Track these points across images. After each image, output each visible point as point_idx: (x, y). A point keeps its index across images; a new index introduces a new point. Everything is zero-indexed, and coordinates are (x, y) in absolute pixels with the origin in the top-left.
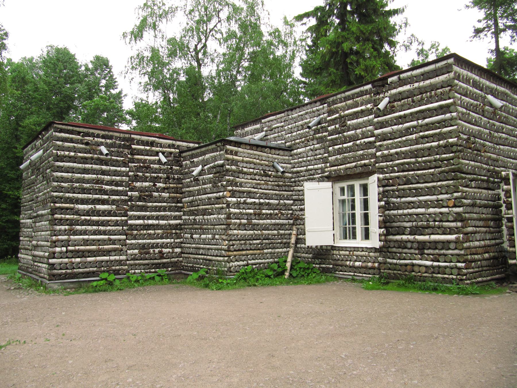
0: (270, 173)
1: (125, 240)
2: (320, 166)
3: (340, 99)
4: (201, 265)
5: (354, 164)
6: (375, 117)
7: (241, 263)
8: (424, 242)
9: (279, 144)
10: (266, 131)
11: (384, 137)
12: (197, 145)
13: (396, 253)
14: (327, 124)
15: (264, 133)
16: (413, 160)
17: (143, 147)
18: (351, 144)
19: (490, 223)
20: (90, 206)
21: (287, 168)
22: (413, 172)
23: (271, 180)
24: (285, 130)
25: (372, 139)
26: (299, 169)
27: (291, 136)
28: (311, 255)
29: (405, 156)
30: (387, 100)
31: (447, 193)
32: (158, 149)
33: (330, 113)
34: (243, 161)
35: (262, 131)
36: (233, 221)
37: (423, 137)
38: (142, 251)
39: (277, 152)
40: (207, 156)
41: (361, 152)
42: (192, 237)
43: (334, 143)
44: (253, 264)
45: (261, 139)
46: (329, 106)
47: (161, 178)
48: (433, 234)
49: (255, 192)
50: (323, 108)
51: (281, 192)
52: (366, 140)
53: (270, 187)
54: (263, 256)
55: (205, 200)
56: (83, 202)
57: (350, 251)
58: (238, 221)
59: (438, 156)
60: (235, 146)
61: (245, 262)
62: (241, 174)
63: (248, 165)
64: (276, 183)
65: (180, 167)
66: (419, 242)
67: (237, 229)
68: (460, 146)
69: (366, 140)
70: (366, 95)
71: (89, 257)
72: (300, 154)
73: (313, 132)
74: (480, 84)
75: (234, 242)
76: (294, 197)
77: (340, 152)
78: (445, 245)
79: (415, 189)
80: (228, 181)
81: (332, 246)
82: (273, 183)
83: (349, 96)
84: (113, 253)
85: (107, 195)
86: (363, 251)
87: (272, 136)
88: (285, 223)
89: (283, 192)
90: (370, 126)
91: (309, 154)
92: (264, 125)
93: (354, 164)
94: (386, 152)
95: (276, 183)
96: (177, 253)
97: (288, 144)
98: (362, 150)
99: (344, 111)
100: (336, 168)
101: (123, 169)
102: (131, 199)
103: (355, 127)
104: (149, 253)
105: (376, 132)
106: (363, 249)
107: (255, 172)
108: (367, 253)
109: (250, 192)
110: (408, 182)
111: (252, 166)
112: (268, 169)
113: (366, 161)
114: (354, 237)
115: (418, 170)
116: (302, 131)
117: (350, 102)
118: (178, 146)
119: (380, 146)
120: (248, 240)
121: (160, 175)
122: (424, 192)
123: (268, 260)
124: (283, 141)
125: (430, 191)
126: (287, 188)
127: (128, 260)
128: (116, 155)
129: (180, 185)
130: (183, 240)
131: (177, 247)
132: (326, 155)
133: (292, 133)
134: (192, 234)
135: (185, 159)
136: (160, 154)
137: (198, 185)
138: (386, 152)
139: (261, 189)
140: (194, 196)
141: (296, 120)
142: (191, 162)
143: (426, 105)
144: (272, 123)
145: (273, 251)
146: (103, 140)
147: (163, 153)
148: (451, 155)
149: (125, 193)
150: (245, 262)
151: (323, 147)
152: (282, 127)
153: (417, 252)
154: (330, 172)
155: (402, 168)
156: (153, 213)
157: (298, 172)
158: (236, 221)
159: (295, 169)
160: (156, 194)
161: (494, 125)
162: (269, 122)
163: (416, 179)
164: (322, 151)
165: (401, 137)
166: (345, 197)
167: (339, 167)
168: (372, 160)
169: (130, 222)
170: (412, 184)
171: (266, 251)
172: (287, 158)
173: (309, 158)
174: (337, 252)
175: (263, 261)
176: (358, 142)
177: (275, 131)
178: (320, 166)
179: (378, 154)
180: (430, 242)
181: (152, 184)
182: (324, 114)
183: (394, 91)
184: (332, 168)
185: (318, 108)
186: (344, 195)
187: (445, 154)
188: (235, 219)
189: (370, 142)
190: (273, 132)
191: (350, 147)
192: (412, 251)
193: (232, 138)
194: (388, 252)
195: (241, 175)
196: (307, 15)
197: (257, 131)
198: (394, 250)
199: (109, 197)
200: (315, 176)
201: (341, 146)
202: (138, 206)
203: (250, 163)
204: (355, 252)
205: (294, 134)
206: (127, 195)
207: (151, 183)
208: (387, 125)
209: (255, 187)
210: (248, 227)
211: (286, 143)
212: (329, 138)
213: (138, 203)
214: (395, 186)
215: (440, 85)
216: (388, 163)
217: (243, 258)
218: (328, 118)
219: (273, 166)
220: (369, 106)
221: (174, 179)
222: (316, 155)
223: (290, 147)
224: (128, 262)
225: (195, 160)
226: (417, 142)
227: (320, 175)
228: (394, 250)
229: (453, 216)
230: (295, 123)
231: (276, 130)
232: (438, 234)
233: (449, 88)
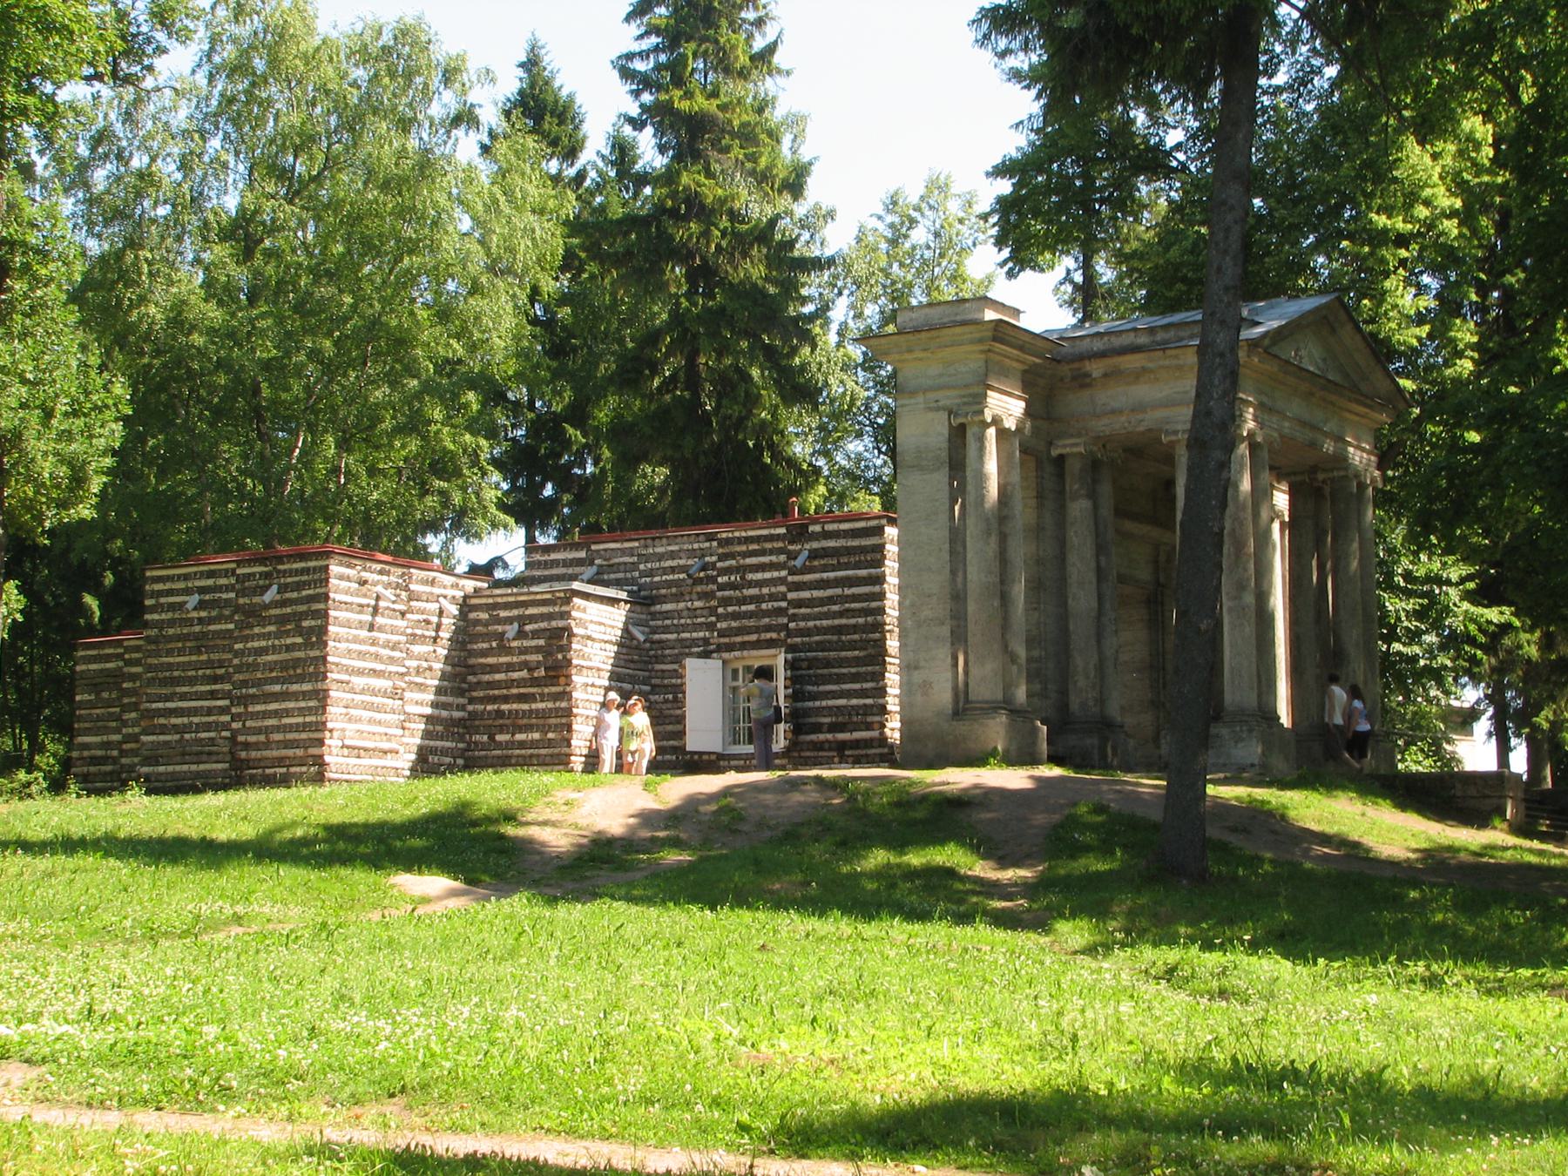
2: (701, 634)
11: (799, 603)
25: (784, 604)
33: (722, 557)
35: (592, 563)
37: (847, 610)
43: (726, 602)
52: (776, 604)
56: (360, 672)
69: (776, 604)
77: (735, 616)
94: (802, 624)
103: (760, 584)
105: (791, 596)
117: (755, 547)
125: (855, 678)
138: (802, 624)
155: (821, 646)
159: (656, 637)
164: (705, 612)
176: (764, 606)
178: (701, 634)
179: (792, 625)
183: (815, 545)
198: (808, 754)
205: (657, 579)
225: (503, 614)
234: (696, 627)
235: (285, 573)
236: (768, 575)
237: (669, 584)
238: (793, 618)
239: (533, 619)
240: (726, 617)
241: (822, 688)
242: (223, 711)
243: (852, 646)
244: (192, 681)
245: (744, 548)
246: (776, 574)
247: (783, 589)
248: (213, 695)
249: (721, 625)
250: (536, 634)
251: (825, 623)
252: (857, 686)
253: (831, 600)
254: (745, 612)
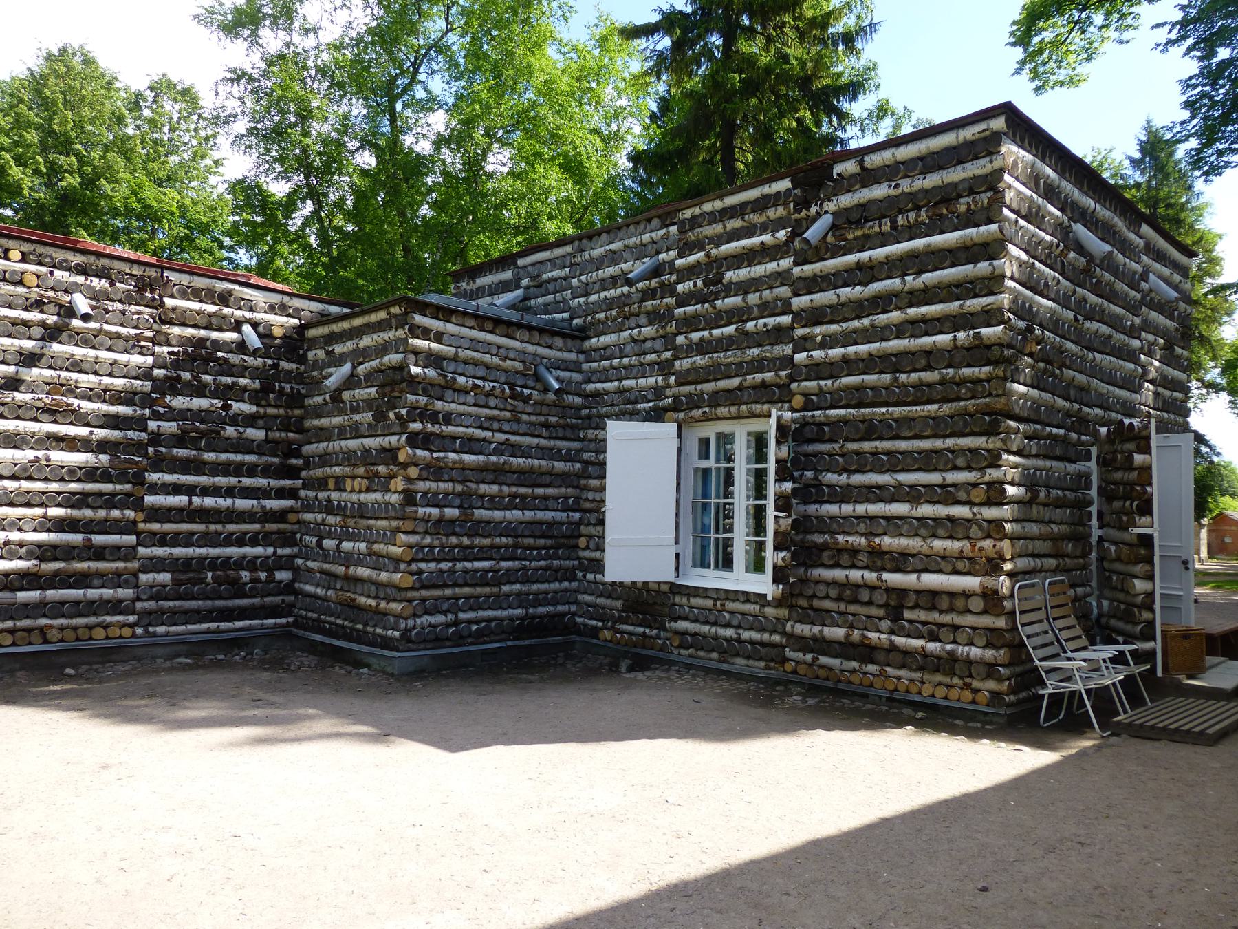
0: (527, 392)
1: (134, 548)
2: (651, 381)
3: (712, 213)
4: (338, 617)
5: (736, 382)
6: (796, 264)
7: (440, 619)
8: (902, 592)
9: (553, 321)
10: (527, 288)
11: (816, 316)
12: (346, 310)
13: (828, 611)
14: (674, 277)
15: (520, 292)
16: (887, 378)
17: (196, 306)
18: (730, 330)
19: (1067, 546)
20: (31, 454)
21: (570, 382)
22: (884, 410)
23: (529, 410)
24: (571, 287)
25: (786, 320)
26: (600, 386)
27: (587, 304)
28: (619, 604)
29: (866, 367)
30: (826, 220)
31: (969, 468)
32: (238, 313)
33: (686, 248)
34: (455, 359)
35: (518, 287)
36: (421, 511)
37: (913, 322)
38: (183, 577)
39: (548, 340)
40: (366, 341)
41: (755, 351)
42: (319, 544)
43: (690, 324)
44: (470, 622)
45: (513, 307)
46: (682, 231)
47: (244, 389)
48: (927, 570)
49: (484, 440)
50: (666, 237)
51: (553, 442)
52: (771, 321)
53: (524, 428)
54: (499, 602)
55: (355, 452)
57: (715, 600)
58: (435, 511)
59: (950, 371)
60: (436, 318)
61: (450, 617)
62: (450, 392)
63: (470, 369)
64: (542, 419)
65: (301, 364)
66: (890, 590)
67: (433, 531)
68: (1009, 346)
69: (771, 321)
70: (775, 205)
71: (22, 589)
72: (604, 349)
73: (640, 295)
74: (1060, 193)
75: (423, 565)
76: (585, 456)
77: (703, 348)
79: (887, 453)
80: (413, 408)
81: (672, 584)
82: (533, 418)
83: (733, 207)
84: (96, 582)
85: (88, 425)
86: (747, 601)
87: (540, 300)
88: (558, 519)
89: (559, 443)
90: (782, 285)
91: (628, 349)
92: (522, 272)
93: (736, 382)
94: (817, 354)
95: (542, 419)
96: (280, 582)
97: (575, 322)
98: (760, 345)
99: (717, 245)
100: (689, 389)
101: (137, 359)
102: (156, 439)
104: (202, 581)
106: (747, 597)
107: (487, 388)
108: (758, 607)
109: (471, 439)
110: (871, 430)
111: (481, 372)
112: (519, 383)
113: (769, 376)
114: (727, 563)
115: (898, 404)
116: (612, 292)
118: (297, 309)
119: (804, 338)
120: (460, 560)
121: (243, 381)
122: (909, 460)
123: (510, 612)
124: (566, 315)
125: (927, 461)
126: (568, 433)
127: (139, 599)
128: (117, 321)
129: (297, 412)
130: (300, 550)
131: (280, 568)
132: (668, 354)
133: (587, 294)
134: (321, 538)
135: (313, 343)
136: (247, 328)
137: (341, 412)
138: (817, 354)
139: (500, 431)
140: (328, 440)
141: (599, 264)
142: (327, 353)
143: (927, 236)
144: (542, 268)
145: (525, 588)
146: (80, 279)
147: (255, 325)
148: (986, 369)
149: (140, 424)
150: (450, 617)
151: (661, 332)
152: (565, 279)
153: (881, 613)
154: (676, 398)
155: (858, 397)
156: (217, 479)
157: (597, 394)
158: (429, 510)
159: (591, 387)
160: (230, 431)
161: (1085, 300)
162: (533, 265)
163: (890, 426)
164: (658, 344)
165: (858, 317)
166: (711, 463)
167: (699, 387)
168: (783, 373)
169: (149, 500)
170: (880, 438)
171: (506, 588)
172: (573, 356)
173: (625, 360)
174: (684, 600)
175: (498, 613)
176: (750, 325)
177: (547, 289)
178: (651, 381)
179: (800, 357)
180: (918, 592)
181: (218, 403)
182: (668, 249)
183: (846, 200)
184: (682, 389)
185: (653, 234)
186: (707, 457)
187: (969, 366)
188: (428, 505)
189: (778, 329)
190: (543, 290)
191: (730, 337)
192: (874, 611)
193: (434, 299)
194: (811, 608)
195: (449, 394)
196: (646, 31)
197: (505, 287)
198: (827, 604)
199: (91, 432)
200: (638, 406)
201: (706, 333)
202: (175, 459)
203: (476, 363)
204: (727, 603)
205: (594, 298)
206: (145, 430)
207: (214, 401)
208: (825, 285)
209: (485, 425)
210: (460, 526)
211: (572, 318)
212: (677, 311)
213: (175, 450)
214: (836, 442)
215: (966, 185)
216: (822, 383)
217: (445, 606)
218: (679, 262)
219: (537, 377)
220: (782, 234)
221: (281, 392)
222: (645, 353)
223: (582, 329)
224: (139, 605)
225: (339, 349)
226: (900, 330)
227: (651, 404)
228: (827, 604)
229: (980, 527)
230: (598, 269)
231: (551, 287)
232: (939, 571)
233: (989, 194)
234: (643, 370)
236: (758, 270)
237: (609, 304)
238: (803, 344)
239: (361, 355)
240: (690, 349)
241: (857, 479)
243: (922, 394)
245: (717, 228)
246: (772, 266)
247: (784, 291)
249: (682, 364)
250: (369, 378)
251: (863, 349)
252: (934, 478)
253: (882, 303)
254: (720, 340)
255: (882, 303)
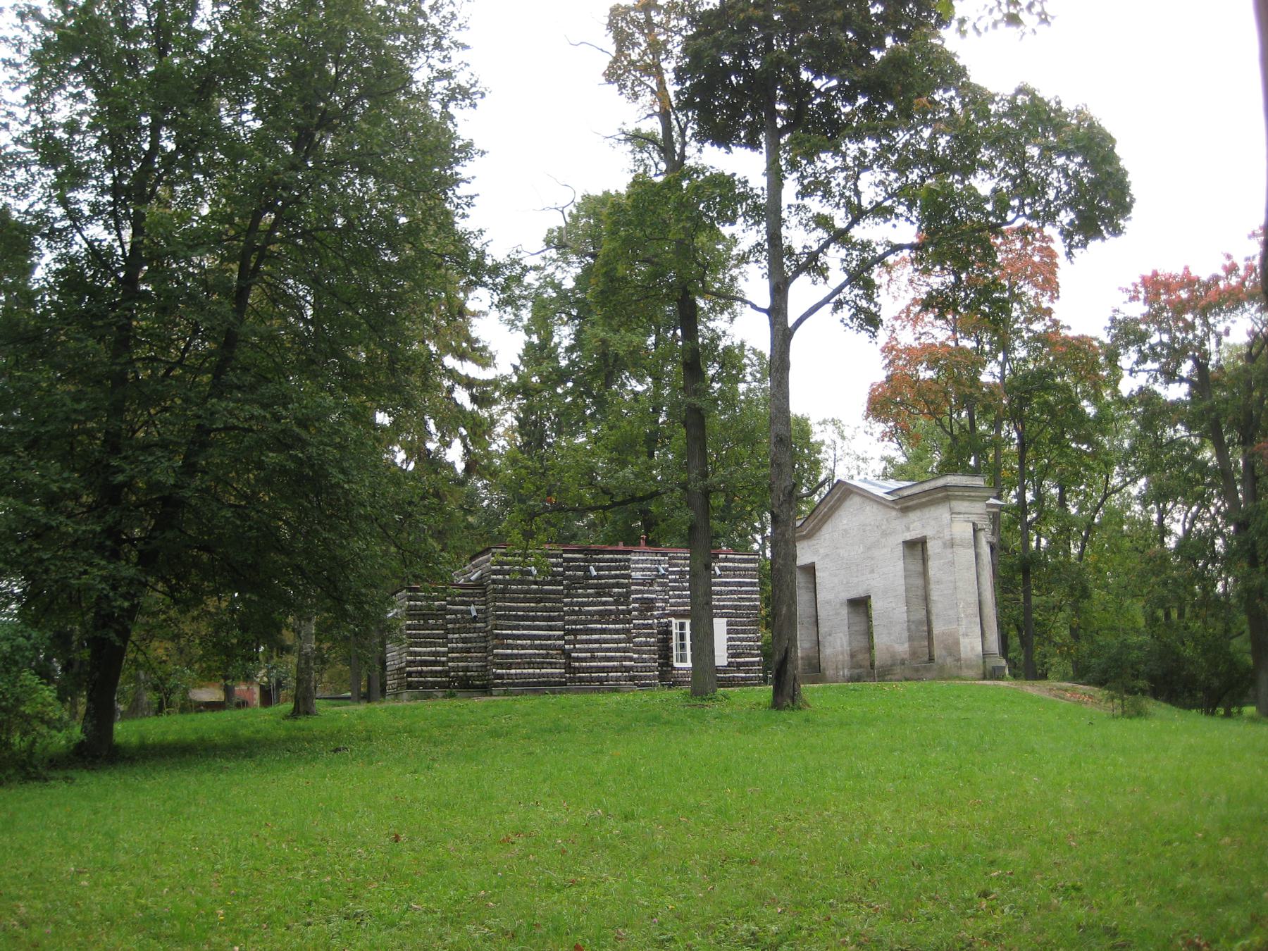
43: (674, 589)
77: (679, 597)
78: (753, 664)
125: (744, 632)
235: (600, 561)
242: (560, 638)
244: (534, 619)
248: (550, 628)
253: (732, 592)
255: (732, 592)
